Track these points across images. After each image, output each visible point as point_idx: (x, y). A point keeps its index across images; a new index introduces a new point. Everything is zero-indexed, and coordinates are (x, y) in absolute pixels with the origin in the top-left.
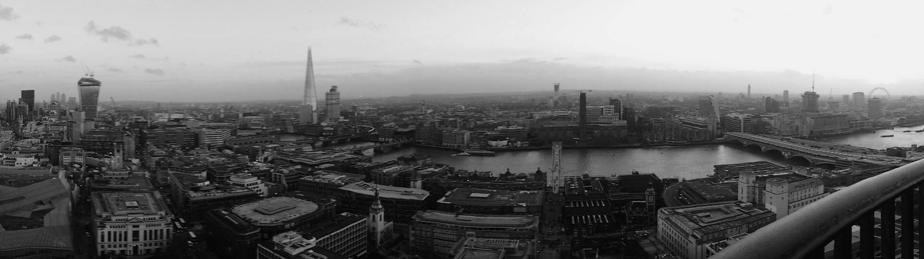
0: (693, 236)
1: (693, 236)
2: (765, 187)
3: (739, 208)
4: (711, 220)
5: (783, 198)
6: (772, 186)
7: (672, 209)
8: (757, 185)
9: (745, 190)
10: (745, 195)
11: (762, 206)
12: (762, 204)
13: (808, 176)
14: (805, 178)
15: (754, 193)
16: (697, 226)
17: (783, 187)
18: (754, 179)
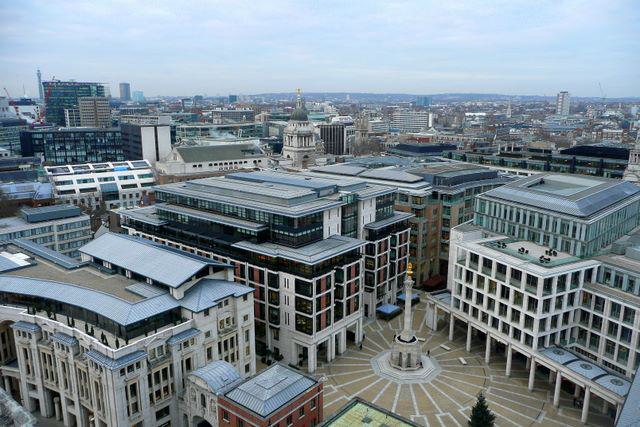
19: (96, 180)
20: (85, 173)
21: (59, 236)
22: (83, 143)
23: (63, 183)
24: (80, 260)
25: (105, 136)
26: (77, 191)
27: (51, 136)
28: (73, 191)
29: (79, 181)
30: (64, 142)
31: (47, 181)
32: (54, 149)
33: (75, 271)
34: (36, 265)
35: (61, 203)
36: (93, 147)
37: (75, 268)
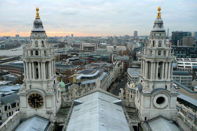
19: (191, 64)
20: (188, 61)
21: (181, 80)
22: (185, 51)
23: (180, 64)
24: (193, 90)
25: (194, 50)
26: (185, 67)
27: (176, 48)
28: (183, 67)
29: (185, 64)
30: (179, 50)
31: (176, 63)
32: (176, 52)
33: (193, 94)
34: (179, 88)
35: (178, 70)
36: (188, 53)
37: (193, 93)
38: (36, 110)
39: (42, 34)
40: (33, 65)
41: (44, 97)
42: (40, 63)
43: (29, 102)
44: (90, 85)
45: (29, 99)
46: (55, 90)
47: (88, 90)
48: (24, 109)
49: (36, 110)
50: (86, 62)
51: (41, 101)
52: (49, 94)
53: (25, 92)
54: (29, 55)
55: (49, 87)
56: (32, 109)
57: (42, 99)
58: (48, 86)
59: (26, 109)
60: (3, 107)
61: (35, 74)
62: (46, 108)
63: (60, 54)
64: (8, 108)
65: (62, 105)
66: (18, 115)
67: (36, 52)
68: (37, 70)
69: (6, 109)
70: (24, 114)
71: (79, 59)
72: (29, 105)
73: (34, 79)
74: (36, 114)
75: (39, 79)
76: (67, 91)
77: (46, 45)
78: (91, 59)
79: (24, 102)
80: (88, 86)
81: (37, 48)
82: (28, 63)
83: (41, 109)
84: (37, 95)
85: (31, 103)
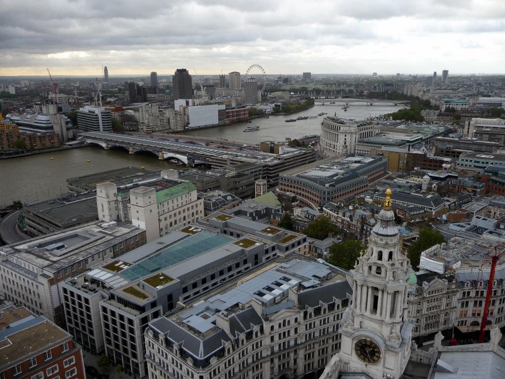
0: (44, 276)
1: (44, 276)
2: (129, 199)
3: (100, 230)
4: (65, 251)
5: (151, 211)
6: (136, 198)
7: (11, 247)
8: (119, 198)
9: (106, 206)
10: (106, 212)
11: (128, 222)
12: (128, 221)
13: (180, 180)
14: (175, 183)
15: (117, 209)
16: (47, 263)
17: (150, 197)
18: (116, 191)
38: (366, 365)
39: (391, 241)
40: (370, 290)
41: (383, 350)
42: (383, 291)
43: (356, 350)
44: (476, 285)
45: (357, 345)
46: (402, 339)
47: (471, 296)
48: (346, 356)
49: (366, 365)
50: (476, 187)
51: (376, 354)
52: (392, 347)
53: (352, 332)
54: (366, 273)
55: (394, 334)
56: (359, 361)
57: (379, 352)
58: (391, 333)
59: (350, 357)
60: (302, 314)
61: (371, 306)
62: (384, 367)
63: (403, 150)
64: (308, 316)
65: (411, 357)
66: (336, 364)
67: (377, 269)
68: (376, 298)
69: (305, 318)
70: (345, 363)
71: (456, 177)
72: (357, 353)
73: (368, 313)
74: (365, 371)
75: (377, 316)
76: (420, 291)
77: (396, 258)
78: (493, 181)
79: (348, 345)
80: (472, 285)
81: (379, 262)
82: (362, 286)
83: (374, 367)
84: (372, 343)
85: (359, 352)
